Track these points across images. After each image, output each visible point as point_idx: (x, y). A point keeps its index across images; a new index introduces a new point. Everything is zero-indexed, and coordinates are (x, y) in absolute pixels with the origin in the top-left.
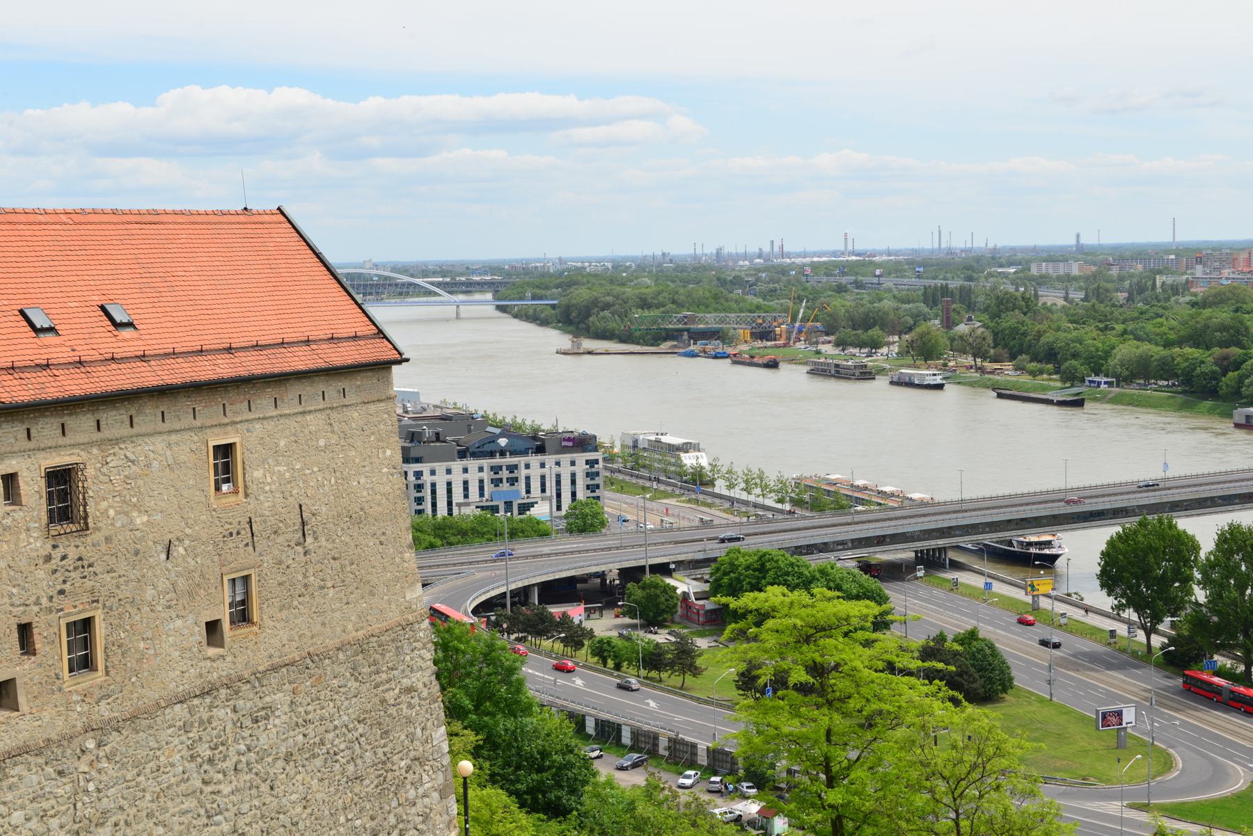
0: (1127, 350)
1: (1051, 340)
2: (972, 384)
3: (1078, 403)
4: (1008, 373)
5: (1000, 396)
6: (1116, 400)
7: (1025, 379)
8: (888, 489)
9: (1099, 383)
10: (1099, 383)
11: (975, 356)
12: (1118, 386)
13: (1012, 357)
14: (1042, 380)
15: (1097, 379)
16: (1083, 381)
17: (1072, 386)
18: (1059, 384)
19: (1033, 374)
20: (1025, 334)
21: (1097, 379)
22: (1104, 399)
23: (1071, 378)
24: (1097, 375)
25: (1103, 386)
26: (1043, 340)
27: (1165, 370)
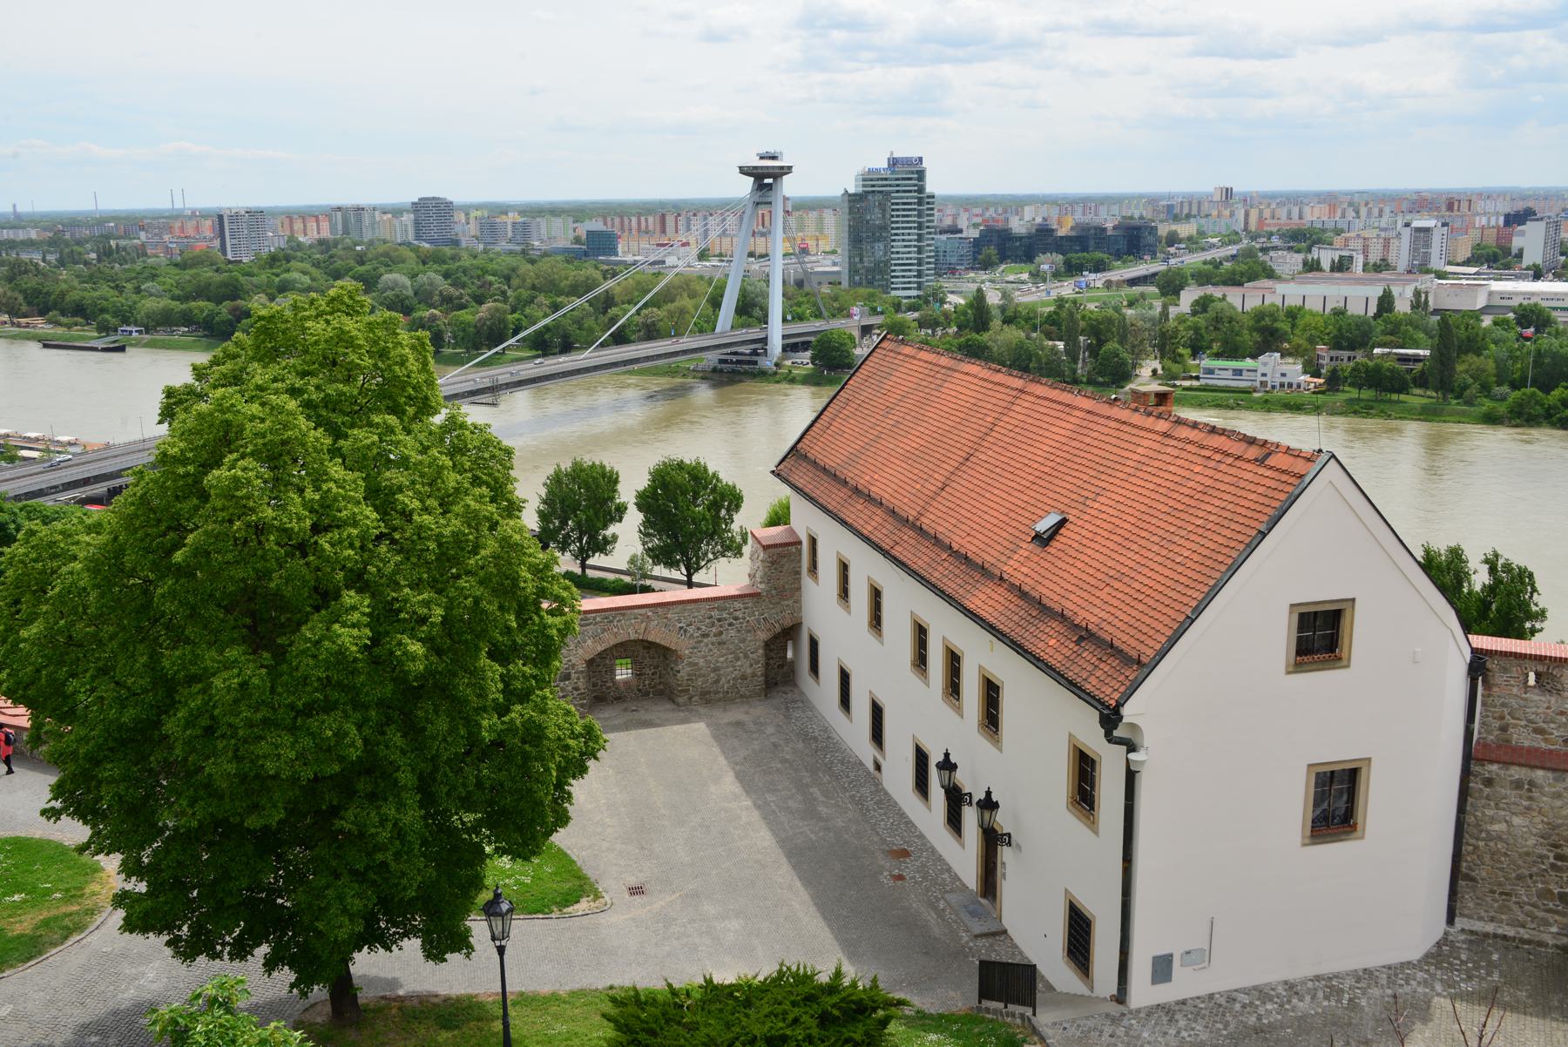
0: (150, 305)
1: (77, 297)
2: (14, 337)
3: (121, 349)
4: (41, 325)
5: (46, 346)
6: (151, 345)
7: (60, 331)
8: (33, 435)
9: (131, 332)
10: (131, 332)
11: (9, 313)
12: (147, 333)
13: (42, 313)
14: (76, 331)
15: (129, 329)
16: (116, 330)
17: (108, 335)
18: (96, 334)
19: (69, 327)
20: (48, 294)
21: (129, 329)
22: (138, 344)
23: (105, 329)
24: (128, 325)
25: (134, 334)
26: (68, 298)
27: (187, 319)
